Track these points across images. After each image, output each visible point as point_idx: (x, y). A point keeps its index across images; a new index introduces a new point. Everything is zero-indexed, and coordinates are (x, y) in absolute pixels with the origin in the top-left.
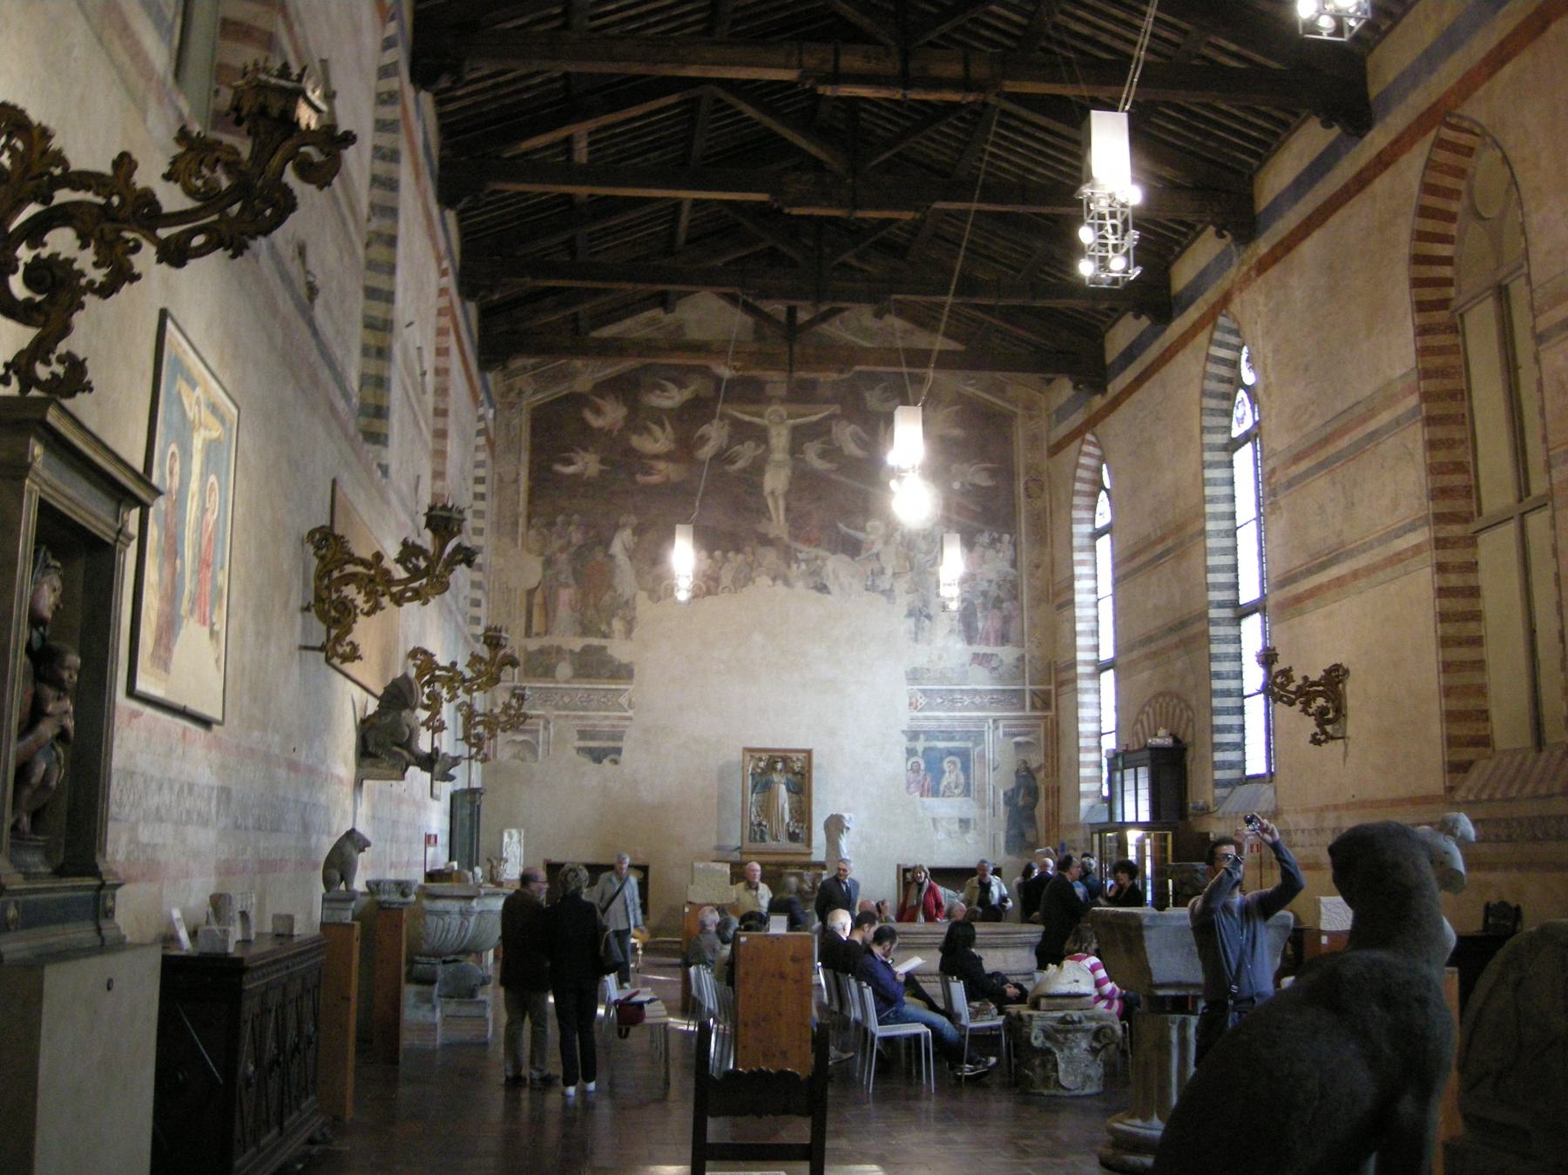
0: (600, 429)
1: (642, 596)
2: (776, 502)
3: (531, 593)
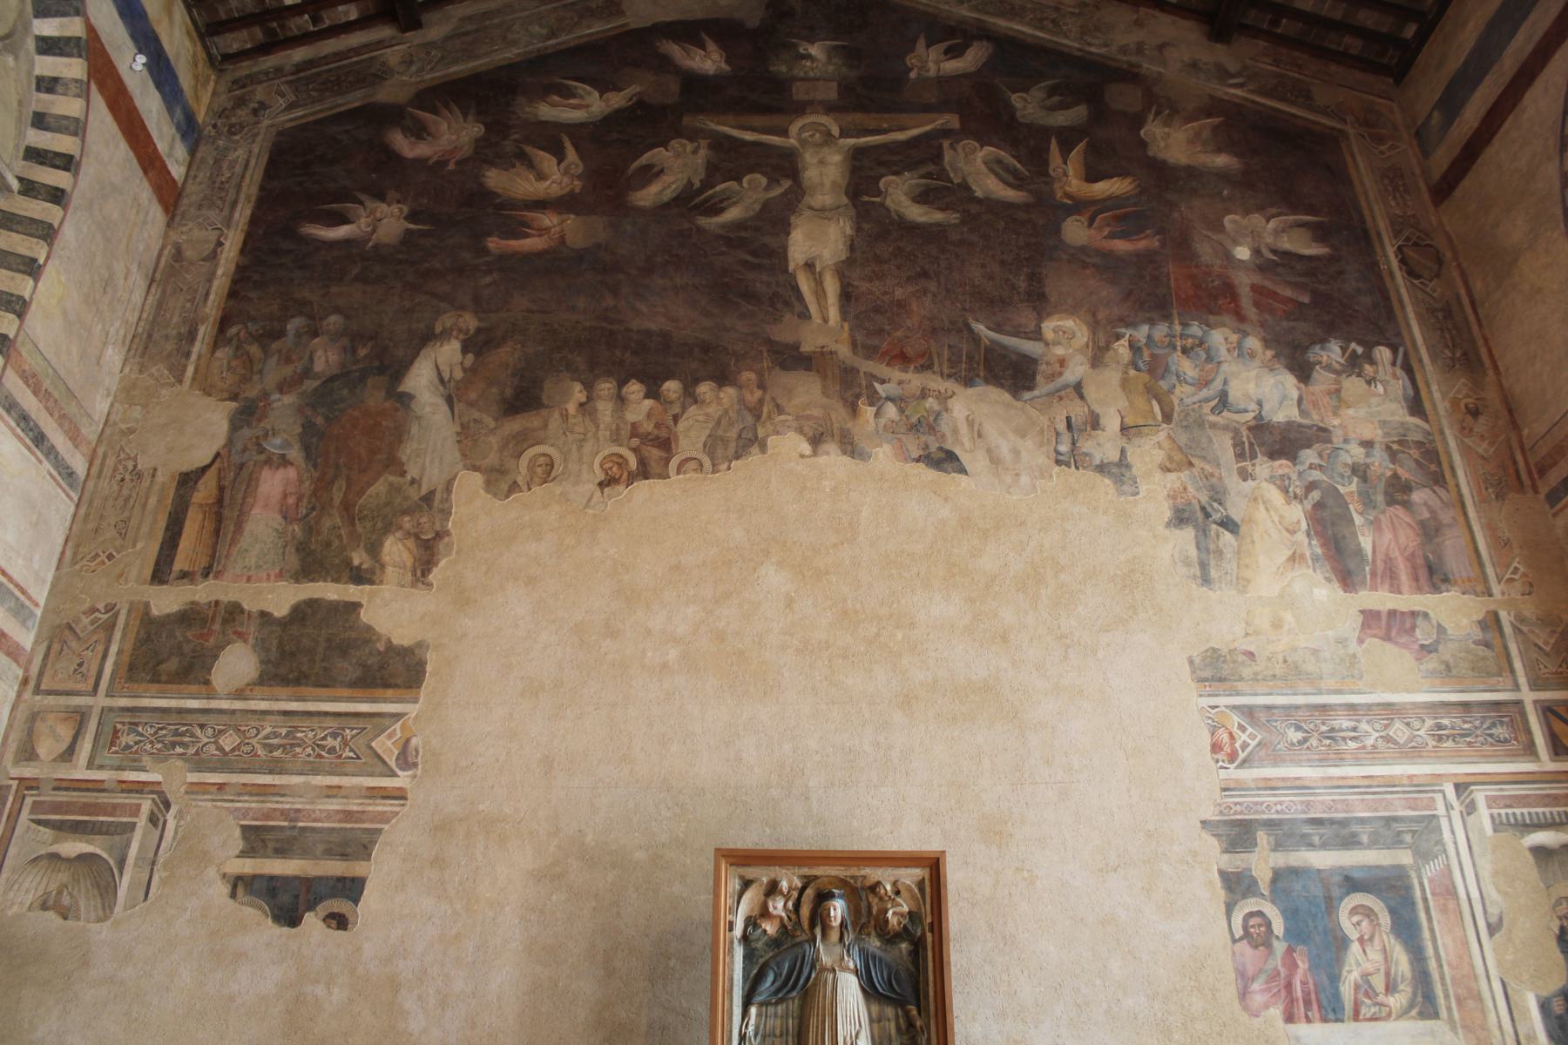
0: (420, 162)
1: (470, 484)
2: (819, 282)
3: (188, 480)
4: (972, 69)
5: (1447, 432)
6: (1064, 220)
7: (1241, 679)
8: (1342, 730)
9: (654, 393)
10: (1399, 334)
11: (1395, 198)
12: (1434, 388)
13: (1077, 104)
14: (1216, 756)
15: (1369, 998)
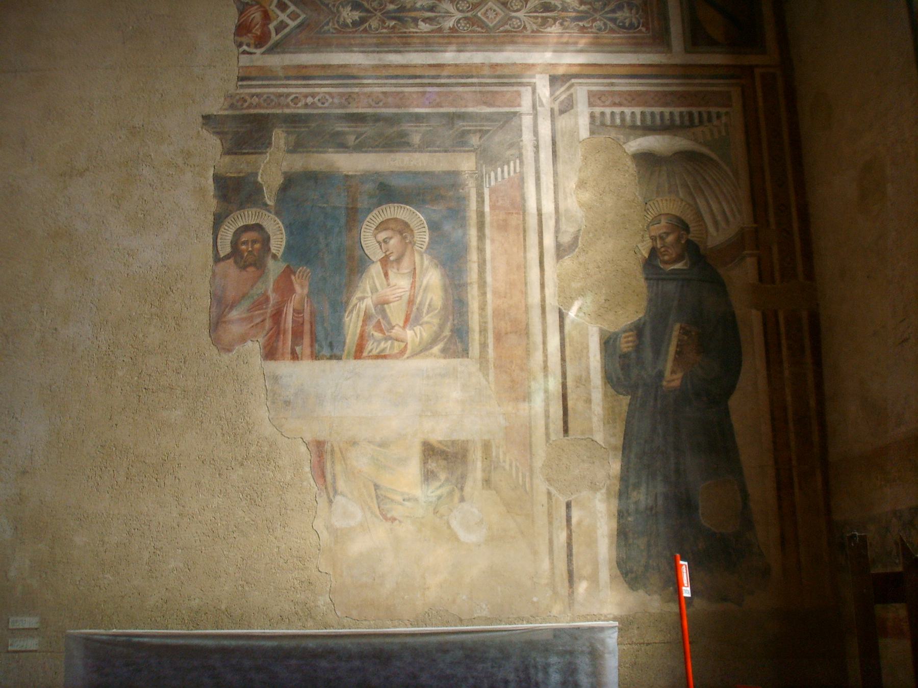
8: (414, 9)
14: (239, 39)
15: (381, 331)
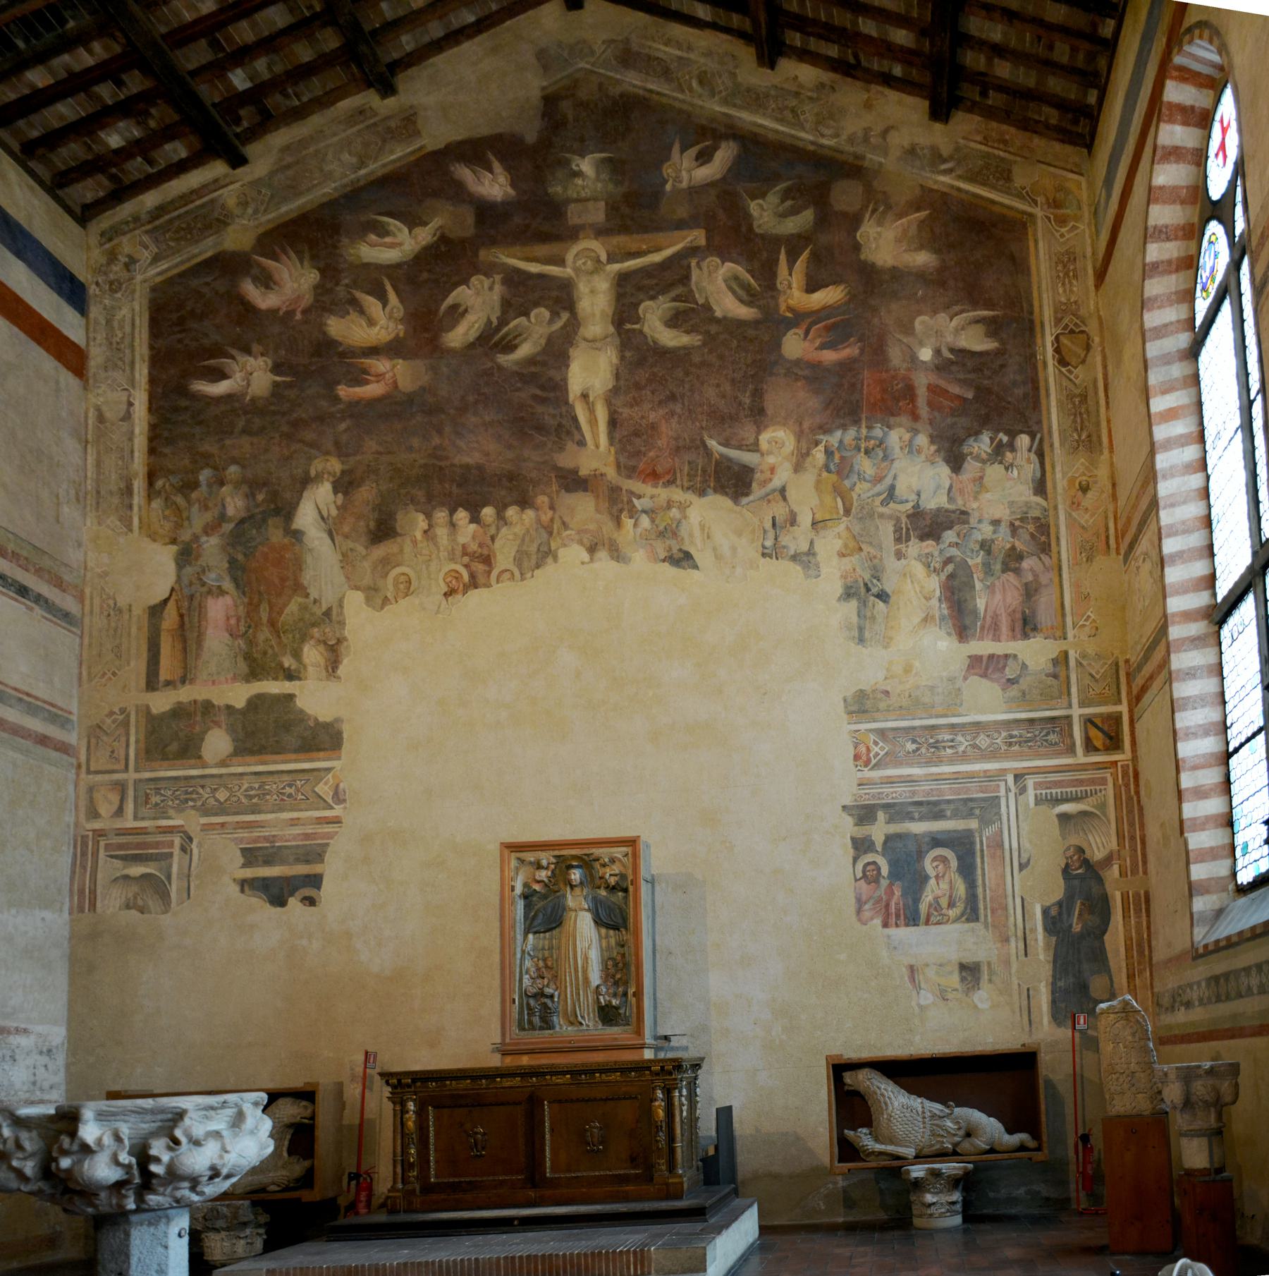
0: (273, 312)
1: (355, 600)
2: (591, 410)
3: (156, 611)
4: (718, 176)
5: (1060, 507)
6: (785, 334)
7: (878, 710)
9: (475, 519)
10: (1039, 422)
11: (1063, 284)
12: (1058, 469)
13: (806, 208)
